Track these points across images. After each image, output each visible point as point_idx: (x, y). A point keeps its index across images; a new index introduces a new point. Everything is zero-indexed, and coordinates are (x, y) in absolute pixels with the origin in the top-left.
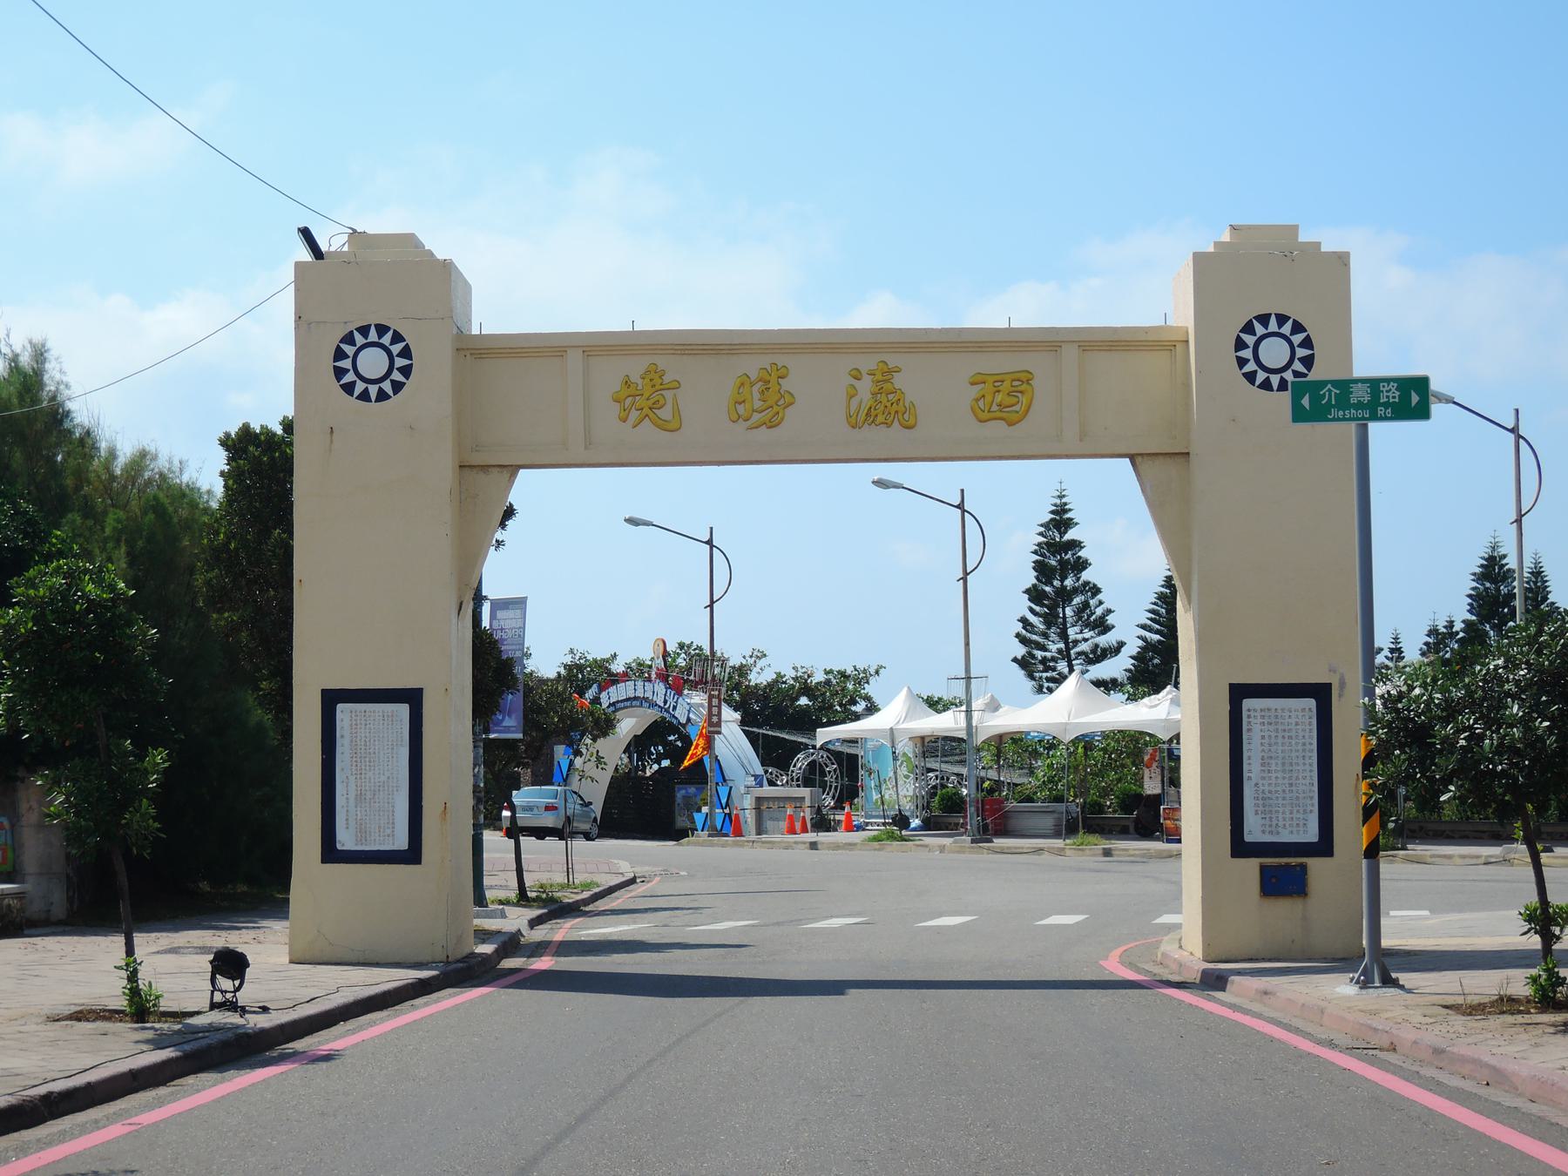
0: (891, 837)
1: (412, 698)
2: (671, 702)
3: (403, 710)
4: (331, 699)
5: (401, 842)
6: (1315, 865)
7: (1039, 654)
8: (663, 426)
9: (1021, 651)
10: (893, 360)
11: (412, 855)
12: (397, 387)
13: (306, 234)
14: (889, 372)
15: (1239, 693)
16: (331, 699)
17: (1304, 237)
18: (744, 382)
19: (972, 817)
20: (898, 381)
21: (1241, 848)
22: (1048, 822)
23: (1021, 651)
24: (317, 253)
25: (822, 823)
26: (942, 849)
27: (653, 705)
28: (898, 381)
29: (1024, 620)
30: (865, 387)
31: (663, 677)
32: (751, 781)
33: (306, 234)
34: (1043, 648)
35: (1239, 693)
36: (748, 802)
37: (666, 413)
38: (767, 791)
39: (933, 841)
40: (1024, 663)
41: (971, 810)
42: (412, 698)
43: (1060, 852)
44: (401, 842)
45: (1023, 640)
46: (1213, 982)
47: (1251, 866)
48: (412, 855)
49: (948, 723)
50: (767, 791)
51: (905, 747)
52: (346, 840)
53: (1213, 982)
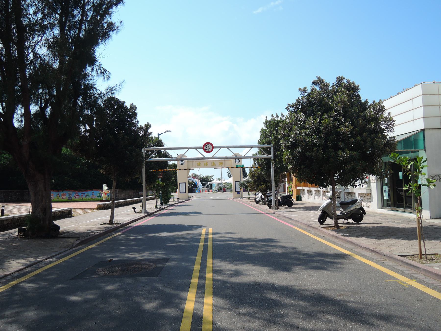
0: (215, 192)
1: (185, 183)
2: (193, 180)
3: (184, 184)
4: (180, 183)
5: (185, 192)
6: (240, 192)
7: (229, 174)
8: (200, 166)
9: (228, 174)
10: (214, 162)
11: (185, 193)
12: (184, 164)
13: (177, 154)
14: (214, 162)
15: (235, 182)
16: (180, 183)
17: (239, 154)
18: (205, 163)
19: (222, 190)
20: (214, 163)
21: (236, 191)
22: (229, 191)
23: (228, 174)
24: (178, 156)
25: (209, 191)
26: (220, 193)
27: (192, 180)
28: (214, 163)
29: (228, 171)
30: (212, 163)
31: (193, 177)
32: (202, 187)
33: (177, 154)
34: (230, 174)
35: (235, 182)
36: (201, 189)
37: (200, 165)
38: (203, 188)
39: (219, 192)
40: (228, 175)
41: (222, 190)
42: (185, 183)
43: (230, 193)
44: (185, 192)
45: (228, 173)
46: (234, 199)
47: (237, 192)
48: (185, 193)
49: (220, 182)
50: (203, 188)
51: (216, 184)
52: (181, 192)
53: (234, 199)
